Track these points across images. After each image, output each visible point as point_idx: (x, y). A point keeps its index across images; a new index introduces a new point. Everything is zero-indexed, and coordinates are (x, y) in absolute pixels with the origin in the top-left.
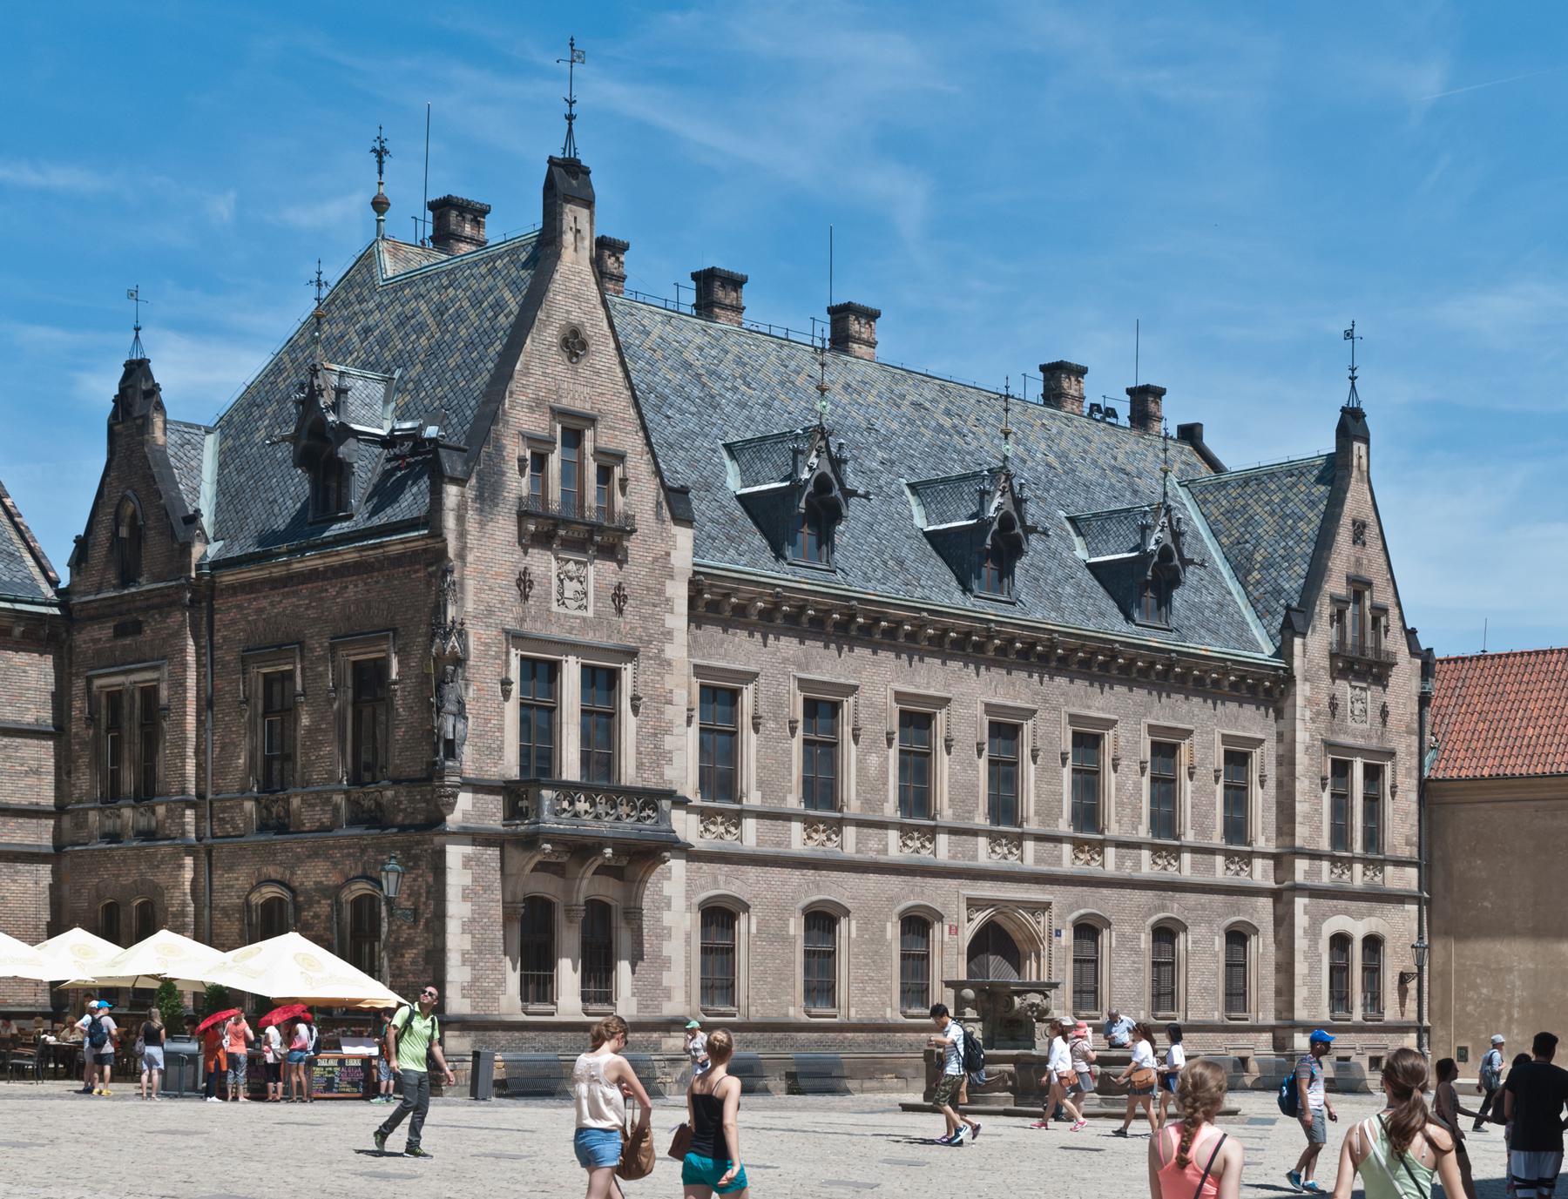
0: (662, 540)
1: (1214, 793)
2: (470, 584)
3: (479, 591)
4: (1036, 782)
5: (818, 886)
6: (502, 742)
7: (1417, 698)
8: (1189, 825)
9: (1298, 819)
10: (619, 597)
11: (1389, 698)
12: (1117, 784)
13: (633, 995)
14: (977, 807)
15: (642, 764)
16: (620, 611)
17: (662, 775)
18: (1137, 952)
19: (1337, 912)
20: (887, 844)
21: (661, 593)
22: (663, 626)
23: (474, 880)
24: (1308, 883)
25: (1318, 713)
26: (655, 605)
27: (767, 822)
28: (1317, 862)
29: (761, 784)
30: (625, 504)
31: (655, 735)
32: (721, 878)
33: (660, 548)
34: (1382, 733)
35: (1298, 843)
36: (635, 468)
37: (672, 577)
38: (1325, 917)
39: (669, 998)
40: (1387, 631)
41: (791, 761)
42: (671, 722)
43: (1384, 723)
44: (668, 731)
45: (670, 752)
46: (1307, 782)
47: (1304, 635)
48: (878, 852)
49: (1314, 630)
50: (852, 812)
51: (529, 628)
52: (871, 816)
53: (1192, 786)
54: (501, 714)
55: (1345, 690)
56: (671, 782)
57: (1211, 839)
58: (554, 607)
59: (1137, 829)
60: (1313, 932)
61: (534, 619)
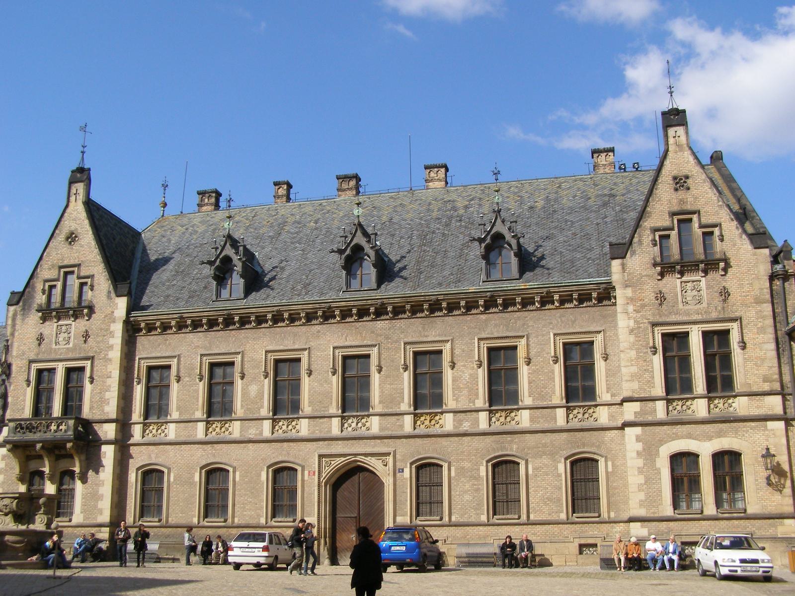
0: (110, 307)
1: (553, 372)
2: (16, 345)
3: (19, 346)
4: (380, 385)
5: (214, 455)
6: (24, 406)
7: (767, 278)
8: (526, 393)
9: (625, 378)
10: (86, 336)
11: (727, 285)
12: (453, 377)
13: (81, 513)
14: (331, 403)
15: (93, 407)
16: (85, 342)
17: (103, 411)
18: (478, 478)
19: (677, 437)
20: (262, 430)
21: (107, 330)
22: (108, 344)
23: (6, 465)
24: (637, 420)
25: (643, 306)
26: (104, 336)
27: (182, 425)
28: (650, 404)
29: (178, 409)
30: (92, 296)
31: (101, 393)
32: (153, 456)
33: (108, 311)
34: (723, 308)
35: (626, 394)
36: (99, 279)
37: (114, 322)
38: (662, 442)
39: (101, 514)
40: (722, 240)
41: (198, 395)
42: (110, 386)
43: (725, 301)
44: (108, 390)
45: (108, 399)
46: (633, 353)
47: (624, 257)
48: (256, 435)
49: (634, 253)
50: (238, 416)
51: (41, 357)
52: (251, 416)
53: (529, 369)
54: (25, 395)
55: (673, 282)
56: (108, 413)
57: (551, 401)
58: (54, 346)
59: (474, 403)
60: (649, 453)
61: (44, 353)
